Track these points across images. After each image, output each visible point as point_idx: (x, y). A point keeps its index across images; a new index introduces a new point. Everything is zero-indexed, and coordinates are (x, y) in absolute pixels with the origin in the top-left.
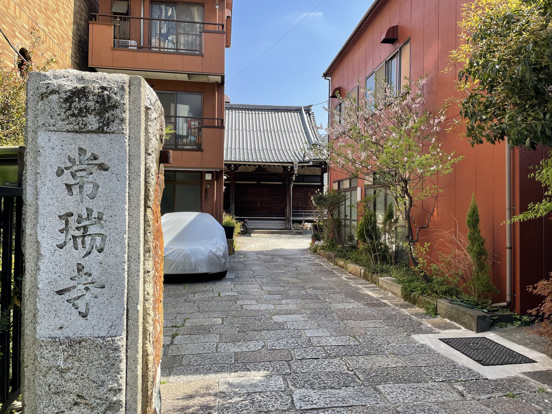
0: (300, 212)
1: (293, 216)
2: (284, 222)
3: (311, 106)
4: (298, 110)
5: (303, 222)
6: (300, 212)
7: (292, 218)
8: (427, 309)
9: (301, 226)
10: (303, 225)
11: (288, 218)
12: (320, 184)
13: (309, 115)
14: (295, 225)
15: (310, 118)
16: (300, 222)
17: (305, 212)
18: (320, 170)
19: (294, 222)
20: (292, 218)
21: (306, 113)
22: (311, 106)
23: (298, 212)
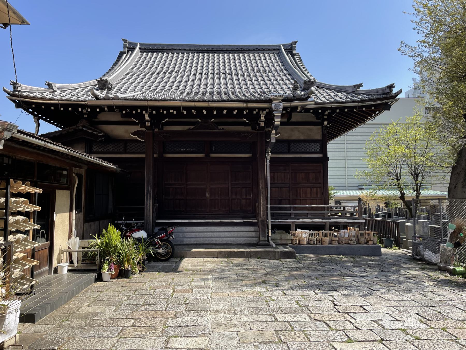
0: (285, 209)
1: (274, 216)
2: (256, 228)
3: (295, 43)
4: (275, 50)
5: (293, 228)
6: (285, 209)
7: (270, 221)
8: (294, 83)
9: (290, 237)
10: (294, 235)
11: (263, 221)
12: (320, 156)
13: (293, 55)
14: (278, 235)
15: (294, 59)
16: (287, 228)
17: (295, 209)
18: (320, 131)
19: (275, 227)
20: (270, 221)
21: (287, 54)
22: (295, 43)
23: (280, 209)
